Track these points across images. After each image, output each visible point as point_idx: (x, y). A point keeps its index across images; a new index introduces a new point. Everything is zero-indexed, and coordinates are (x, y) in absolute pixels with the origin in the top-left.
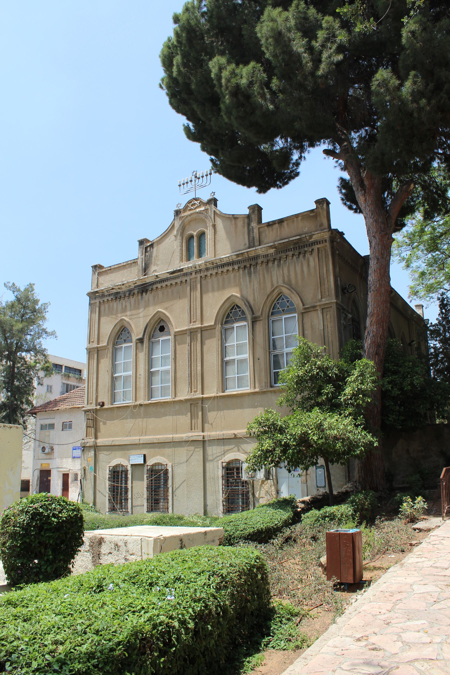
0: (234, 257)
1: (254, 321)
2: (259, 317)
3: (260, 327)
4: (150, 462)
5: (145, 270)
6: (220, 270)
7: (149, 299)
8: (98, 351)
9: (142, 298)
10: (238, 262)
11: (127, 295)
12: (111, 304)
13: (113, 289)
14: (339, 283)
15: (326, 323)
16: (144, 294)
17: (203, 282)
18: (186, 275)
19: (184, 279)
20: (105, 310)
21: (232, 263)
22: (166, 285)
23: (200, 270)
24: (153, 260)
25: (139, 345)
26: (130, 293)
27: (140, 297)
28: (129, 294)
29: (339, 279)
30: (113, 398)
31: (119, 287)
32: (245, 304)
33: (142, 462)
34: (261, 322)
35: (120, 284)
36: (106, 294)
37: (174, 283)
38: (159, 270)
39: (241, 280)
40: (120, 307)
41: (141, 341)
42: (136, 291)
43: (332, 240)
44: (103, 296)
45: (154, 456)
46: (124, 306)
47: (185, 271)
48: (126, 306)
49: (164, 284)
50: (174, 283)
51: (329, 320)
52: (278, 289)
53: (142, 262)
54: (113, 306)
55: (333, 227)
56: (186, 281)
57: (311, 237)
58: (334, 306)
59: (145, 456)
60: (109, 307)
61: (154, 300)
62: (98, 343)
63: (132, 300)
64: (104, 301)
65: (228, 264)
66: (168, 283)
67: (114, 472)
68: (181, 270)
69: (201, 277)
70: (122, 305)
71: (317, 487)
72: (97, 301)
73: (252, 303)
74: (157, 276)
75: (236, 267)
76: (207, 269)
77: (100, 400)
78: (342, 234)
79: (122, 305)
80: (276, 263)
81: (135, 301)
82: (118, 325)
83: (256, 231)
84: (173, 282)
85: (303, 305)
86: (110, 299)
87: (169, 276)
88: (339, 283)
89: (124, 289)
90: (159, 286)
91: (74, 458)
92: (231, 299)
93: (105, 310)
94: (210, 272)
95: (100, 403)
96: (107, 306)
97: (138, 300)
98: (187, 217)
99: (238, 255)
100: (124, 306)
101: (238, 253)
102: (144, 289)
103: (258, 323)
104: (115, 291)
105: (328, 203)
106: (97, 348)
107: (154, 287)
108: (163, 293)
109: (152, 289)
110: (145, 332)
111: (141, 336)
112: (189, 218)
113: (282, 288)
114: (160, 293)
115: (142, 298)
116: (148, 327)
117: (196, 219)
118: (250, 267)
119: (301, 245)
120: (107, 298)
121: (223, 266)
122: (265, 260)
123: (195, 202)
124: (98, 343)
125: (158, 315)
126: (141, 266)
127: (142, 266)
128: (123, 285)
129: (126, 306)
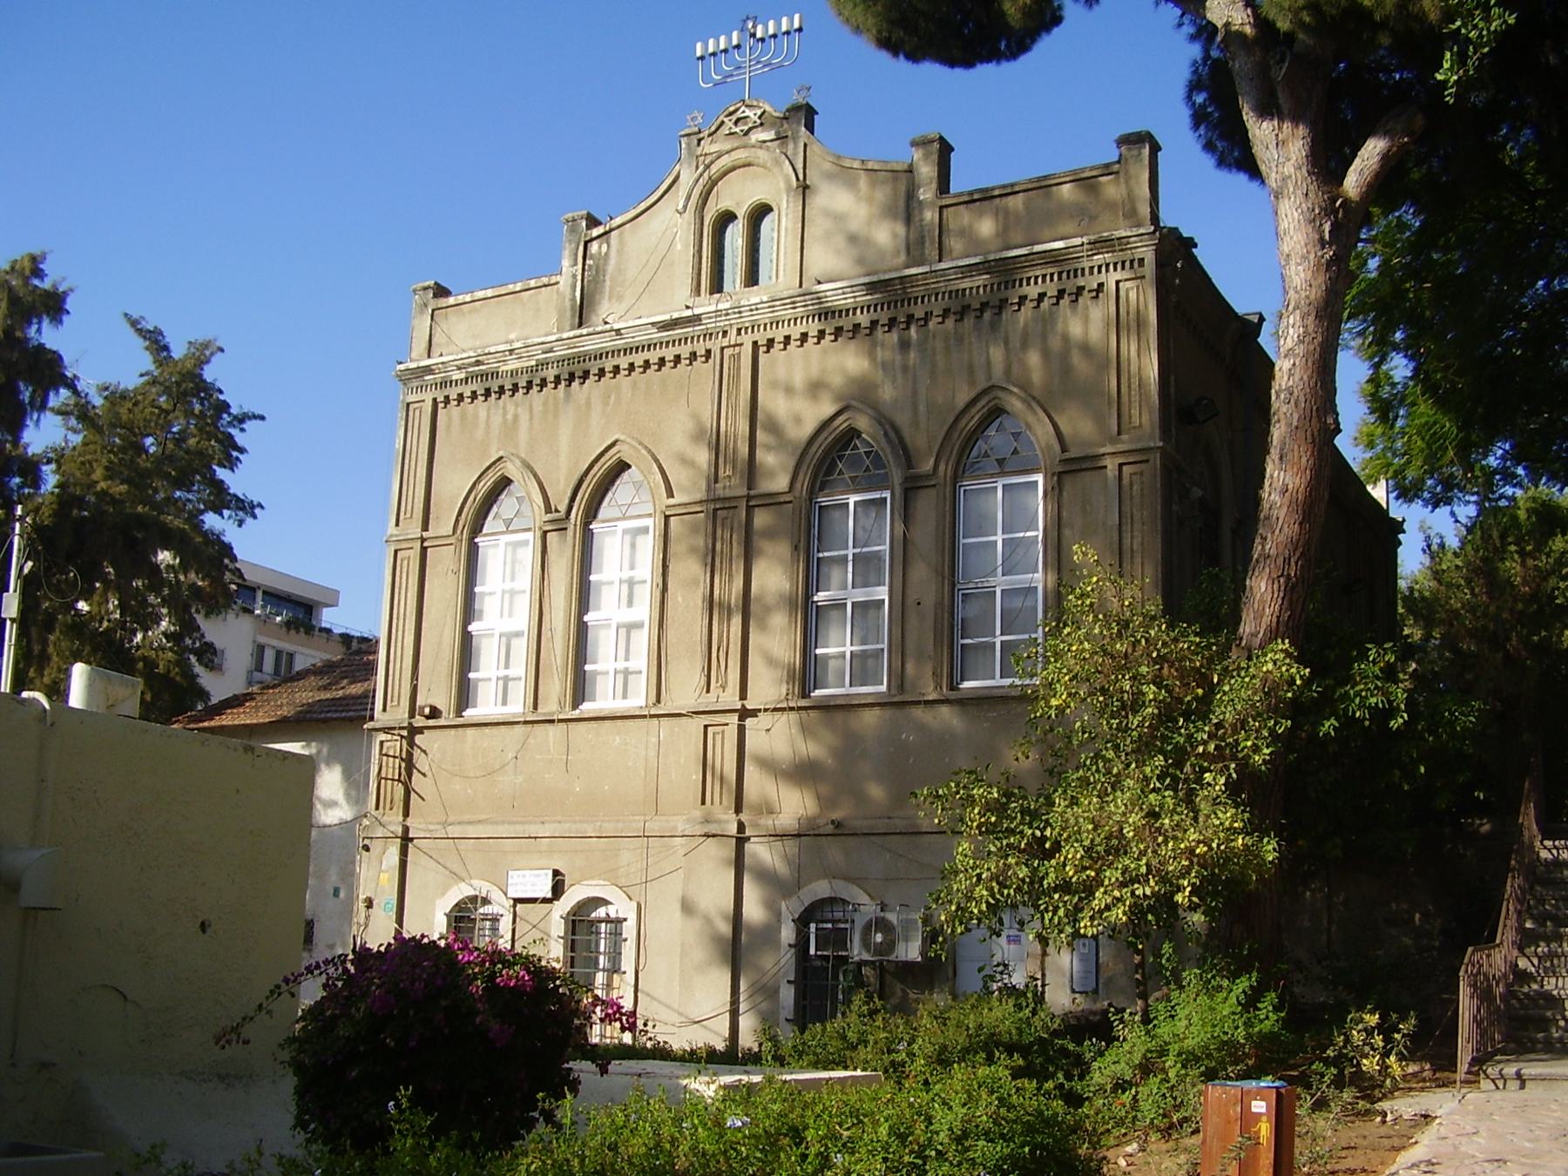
1: (911, 489)
2: (927, 476)
3: (926, 505)
5: (582, 314)
7: (588, 403)
8: (424, 550)
9: (568, 396)
11: (523, 383)
13: (478, 363)
14: (1172, 391)
15: (1126, 508)
16: (575, 384)
17: (762, 358)
18: (708, 335)
20: (449, 427)
24: (608, 283)
26: (533, 382)
28: (530, 383)
29: (1172, 378)
30: (464, 694)
32: (886, 434)
33: (549, 895)
34: (932, 492)
36: (458, 376)
37: (670, 357)
40: (497, 420)
42: (550, 374)
43: (1162, 263)
44: (445, 383)
45: (583, 877)
47: (709, 324)
48: (516, 417)
49: (638, 359)
51: (1137, 500)
54: (476, 417)
55: (1167, 220)
56: (709, 352)
59: (556, 873)
60: (463, 417)
61: (606, 404)
62: (425, 527)
64: (447, 397)
66: (653, 357)
67: (458, 919)
68: (696, 319)
69: (755, 343)
70: (505, 414)
74: (618, 332)
78: (1190, 243)
79: (505, 414)
80: (987, 315)
81: (545, 404)
83: (930, 215)
84: (669, 353)
85: (1064, 450)
88: (1172, 391)
93: (449, 427)
95: (422, 708)
100: (509, 417)
101: (875, 278)
102: (576, 371)
103: (923, 493)
105: (1155, 148)
106: (423, 540)
108: (634, 386)
110: (573, 499)
112: (725, 161)
113: (1000, 394)
115: (568, 396)
118: (908, 324)
119: (1067, 268)
120: (459, 389)
122: (956, 307)
123: (748, 113)
124: (425, 527)
126: (568, 297)
128: (511, 351)
129: (516, 417)
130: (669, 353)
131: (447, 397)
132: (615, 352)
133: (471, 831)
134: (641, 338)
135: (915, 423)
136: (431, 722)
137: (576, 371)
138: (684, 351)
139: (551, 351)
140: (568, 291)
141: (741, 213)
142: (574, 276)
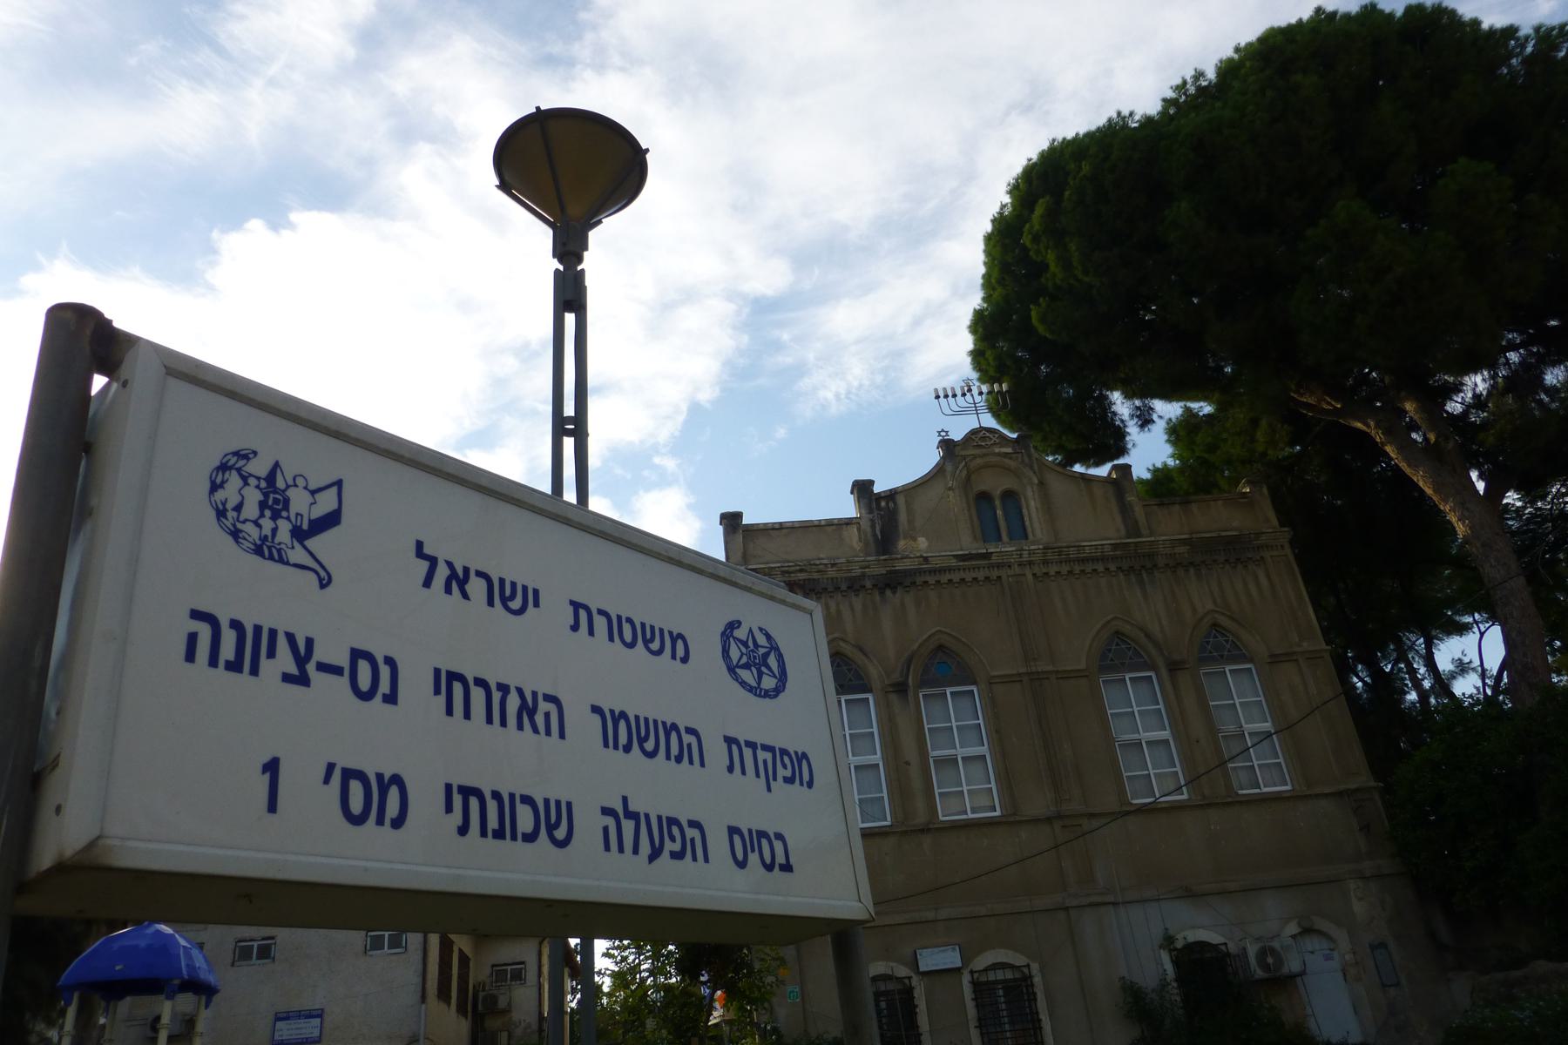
0: (1107, 549)
1: (1174, 667)
4: (982, 962)
6: (1077, 569)
10: (1114, 558)
11: (844, 587)
13: (801, 571)
18: (999, 566)
19: (995, 573)
21: (1103, 559)
23: (1030, 563)
25: (893, 697)
26: (854, 585)
27: (878, 598)
38: (917, 546)
42: (868, 584)
47: (994, 559)
48: (839, 612)
49: (944, 578)
53: (873, 527)
57: (1258, 535)
58: (1327, 657)
63: (857, 602)
65: (1094, 560)
66: (956, 577)
68: (987, 556)
71: (1384, 985)
74: (926, 559)
75: (1113, 567)
76: (1046, 563)
80: (1192, 571)
84: (969, 576)
87: (954, 563)
89: (832, 573)
90: (931, 580)
94: (1053, 570)
98: (975, 457)
99: (1115, 546)
107: (919, 580)
111: (896, 677)
112: (979, 461)
121: (1083, 561)
127: (875, 535)
128: (833, 565)
130: (969, 576)
132: (920, 572)
137: (892, 582)
138: (981, 575)
140: (869, 530)
141: (997, 493)
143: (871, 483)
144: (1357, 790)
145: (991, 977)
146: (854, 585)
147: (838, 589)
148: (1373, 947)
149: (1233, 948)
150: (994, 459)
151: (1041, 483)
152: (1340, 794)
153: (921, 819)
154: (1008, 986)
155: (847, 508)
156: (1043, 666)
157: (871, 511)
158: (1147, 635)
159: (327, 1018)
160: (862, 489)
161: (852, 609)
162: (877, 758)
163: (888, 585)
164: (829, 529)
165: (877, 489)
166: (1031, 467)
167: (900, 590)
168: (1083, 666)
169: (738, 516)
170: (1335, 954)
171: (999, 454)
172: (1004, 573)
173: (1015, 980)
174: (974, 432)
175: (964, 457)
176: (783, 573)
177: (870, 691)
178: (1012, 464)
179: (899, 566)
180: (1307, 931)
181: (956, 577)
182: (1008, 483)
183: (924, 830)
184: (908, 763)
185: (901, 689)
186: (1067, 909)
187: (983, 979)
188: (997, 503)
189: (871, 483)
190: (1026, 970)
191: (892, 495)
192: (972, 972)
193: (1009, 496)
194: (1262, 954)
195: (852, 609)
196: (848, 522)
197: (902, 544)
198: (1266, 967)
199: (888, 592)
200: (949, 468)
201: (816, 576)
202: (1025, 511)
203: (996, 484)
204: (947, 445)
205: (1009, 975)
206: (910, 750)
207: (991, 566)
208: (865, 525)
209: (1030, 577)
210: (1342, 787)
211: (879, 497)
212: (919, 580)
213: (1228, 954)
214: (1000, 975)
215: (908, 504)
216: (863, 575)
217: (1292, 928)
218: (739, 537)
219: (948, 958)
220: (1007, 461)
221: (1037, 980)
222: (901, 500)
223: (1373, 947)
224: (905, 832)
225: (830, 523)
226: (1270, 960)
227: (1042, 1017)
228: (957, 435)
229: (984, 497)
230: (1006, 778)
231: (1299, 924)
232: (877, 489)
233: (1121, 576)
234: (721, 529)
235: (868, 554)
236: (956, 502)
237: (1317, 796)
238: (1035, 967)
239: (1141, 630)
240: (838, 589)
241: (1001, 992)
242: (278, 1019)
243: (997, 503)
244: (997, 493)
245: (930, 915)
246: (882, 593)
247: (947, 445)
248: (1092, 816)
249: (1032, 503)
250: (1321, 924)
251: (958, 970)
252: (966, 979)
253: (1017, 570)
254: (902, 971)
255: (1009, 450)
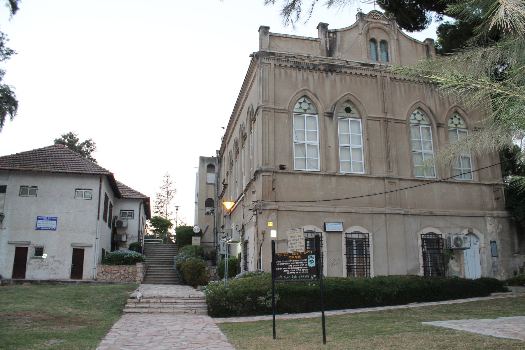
2: (443, 124)
9: (327, 76)
11: (311, 68)
12: (289, 71)
13: (294, 57)
22: (356, 73)
24: (337, 47)
25: (327, 119)
27: (325, 74)
31: (303, 57)
35: (305, 55)
37: (364, 74)
39: (425, 92)
41: (330, 115)
42: (322, 68)
45: (351, 225)
46: (305, 77)
48: (308, 78)
49: (354, 72)
50: (364, 74)
52: (454, 109)
53: (326, 44)
54: (291, 74)
61: (341, 82)
63: (316, 75)
64: (280, 65)
66: (359, 72)
68: (373, 66)
71: (492, 256)
72: (272, 62)
73: (434, 112)
74: (347, 62)
77: (279, 164)
81: (319, 77)
82: (300, 93)
86: (289, 65)
89: (307, 61)
90: (348, 71)
91: (40, 229)
92: (418, 104)
96: (283, 71)
97: (323, 77)
98: (372, 23)
100: (305, 77)
104: (294, 60)
106: (275, 109)
107: (343, 70)
108: (351, 79)
109: (341, 72)
111: (329, 110)
112: (373, 25)
114: (348, 78)
115: (327, 76)
116: (337, 105)
117: (379, 28)
125: (347, 96)
127: (327, 48)
128: (308, 57)
130: (364, 73)
131: (280, 65)
133: (306, 209)
134: (355, 65)
135: (436, 110)
136: (285, 171)
137: (331, 69)
138: (369, 73)
139: (322, 61)
140: (324, 45)
141: (379, 40)
142: (326, 41)
143: (328, 25)
144: (497, 184)
145: (353, 236)
146: (315, 68)
147: (308, 68)
148: (491, 242)
149: (444, 237)
150: (380, 25)
151: (398, 40)
152: (490, 185)
153: (332, 171)
154: (358, 240)
155: (314, 34)
156: (389, 116)
157: (326, 37)
158: (431, 111)
159: (58, 220)
160: (323, 26)
161: (313, 78)
162: (317, 143)
163: (330, 70)
164: (307, 42)
165: (330, 28)
166: (395, 32)
167: (334, 73)
168: (405, 119)
169: (267, 28)
170: (478, 243)
171: (382, 24)
172: (378, 74)
173: (361, 238)
174: (373, 12)
175: (367, 21)
176: (286, 57)
177: (317, 114)
178: (387, 29)
179: (336, 63)
180: (470, 233)
181: (359, 72)
182: (384, 37)
183: (334, 176)
184: (330, 147)
185: (330, 115)
186: (386, 214)
187: (350, 236)
188: (379, 44)
189: (328, 25)
190: (367, 235)
191: (335, 32)
192: (346, 234)
193: (383, 42)
194: (457, 239)
195: (313, 78)
196: (316, 40)
197: (337, 54)
198: (457, 245)
199: (329, 73)
200: (361, 25)
201: (300, 61)
202: (389, 50)
203: (379, 36)
204: (361, 15)
205: (360, 236)
206: (331, 142)
207: (374, 70)
208: (323, 42)
209: (389, 78)
210: (492, 182)
211: (330, 32)
212: (343, 70)
213: (442, 239)
214: (357, 236)
215: (341, 37)
216: (320, 64)
217: (465, 232)
218: (267, 38)
219: (339, 227)
220: (384, 27)
221: (371, 239)
222: (339, 34)
223: (491, 242)
224: (326, 175)
225: (308, 39)
226: (459, 242)
227: (370, 253)
228: (366, 12)
229: (373, 41)
230: (369, 159)
231: (468, 231)
232: (330, 28)
233: (424, 84)
234: (258, 34)
235: (322, 55)
236: (362, 41)
237: (483, 184)
238: (370, 234)
239: (429, 108)
240: (308, 68)
241: (354, 243)
242: (38, 219)
243: (379, 44)
244: (379, 40)
245: (332, 209)
246: (327, 73)
247: (361, 15)
248: (400, 179)
249: (393, 47)
250: (475, 231)
251: (341, 232)
252: (344, 236)
253: (383, 74)
254: (319, 230)
255: (386, 23)
